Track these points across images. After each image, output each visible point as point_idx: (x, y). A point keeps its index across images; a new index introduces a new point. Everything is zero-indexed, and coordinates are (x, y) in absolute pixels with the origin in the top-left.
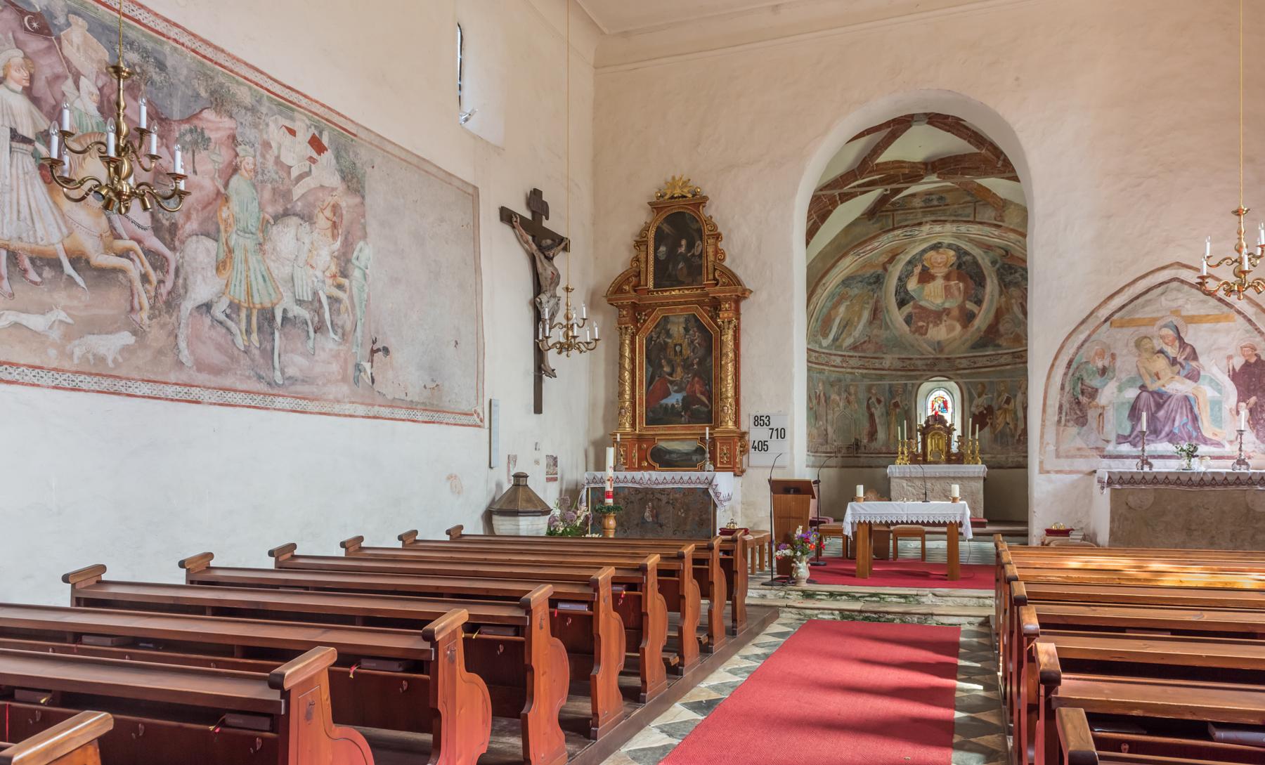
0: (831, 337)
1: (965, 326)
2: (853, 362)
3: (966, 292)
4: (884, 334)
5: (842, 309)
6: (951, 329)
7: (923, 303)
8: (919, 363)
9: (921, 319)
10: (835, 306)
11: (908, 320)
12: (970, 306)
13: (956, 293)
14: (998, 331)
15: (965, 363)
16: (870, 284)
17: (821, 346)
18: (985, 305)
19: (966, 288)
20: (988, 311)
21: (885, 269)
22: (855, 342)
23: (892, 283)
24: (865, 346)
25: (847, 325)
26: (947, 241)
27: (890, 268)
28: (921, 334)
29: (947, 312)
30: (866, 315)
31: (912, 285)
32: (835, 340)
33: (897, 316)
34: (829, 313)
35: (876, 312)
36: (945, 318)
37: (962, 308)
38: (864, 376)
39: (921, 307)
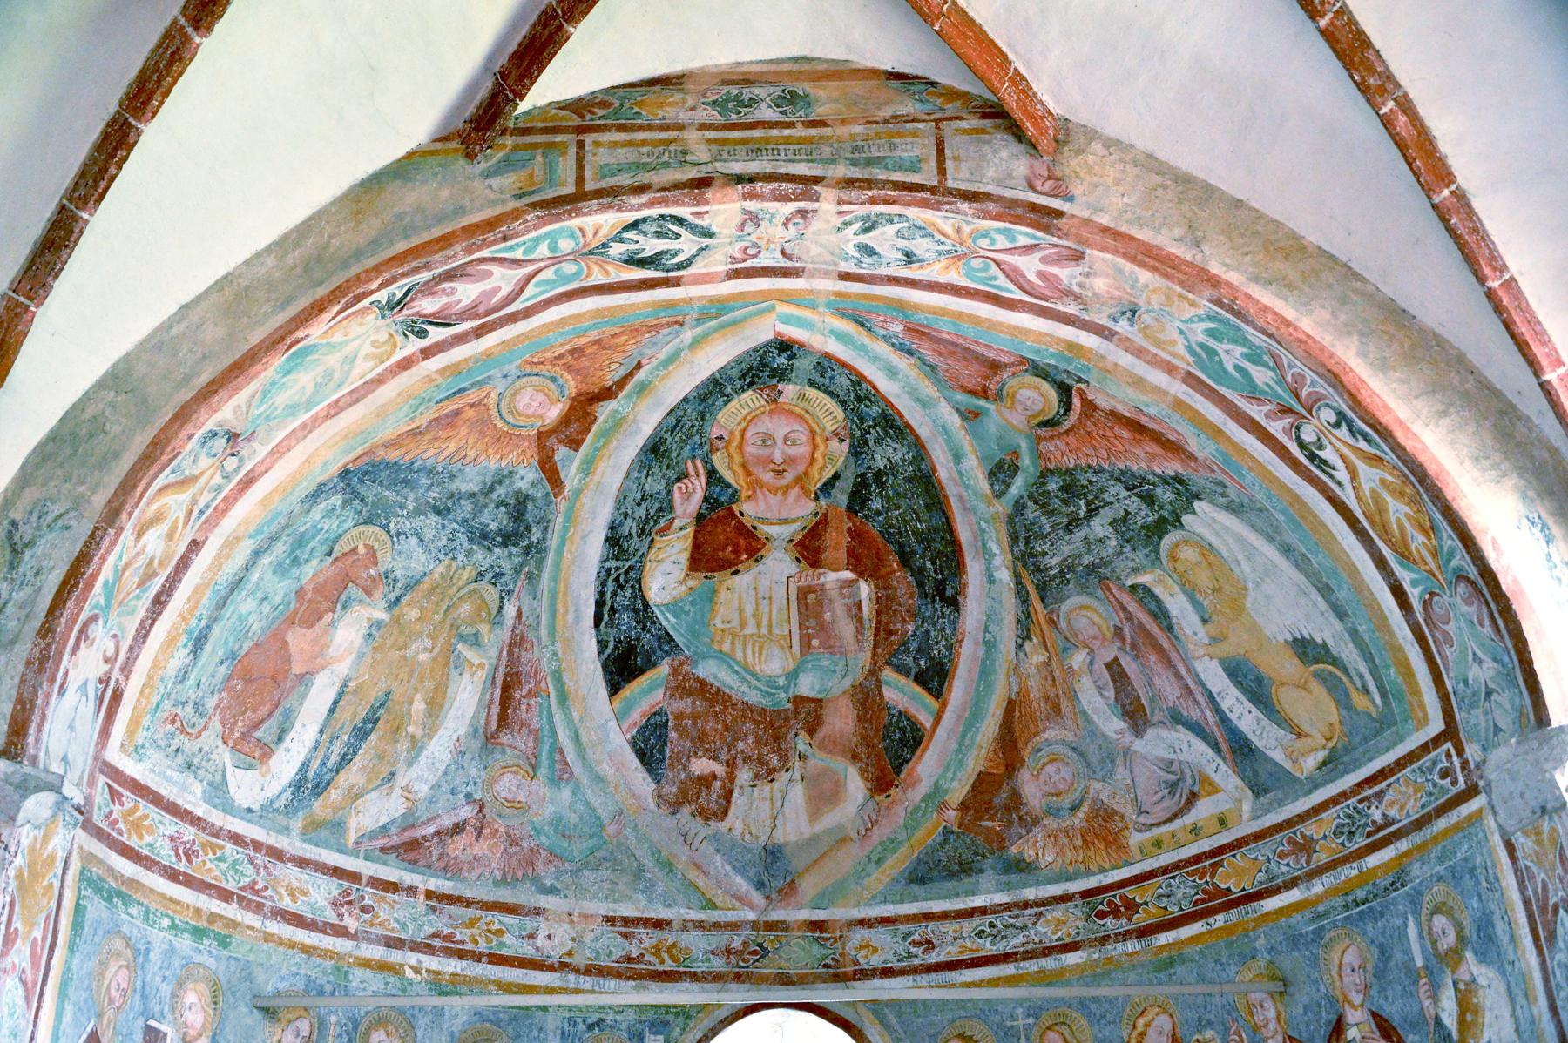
0: (286, 764)
1: (882, 784)
2: (395, 914)
3: (883, 630)
4: (549, 803)
5: (348, 633)
6: (823, 795)
7: (708, 670)
8: (698, 944)
9: (701, 744)
10: (318, 605)
11: (650, 747)
12: (900, 692)
13: (846, 629)
14: (1016, 799)
15: (886, 947)
16: (482, 537)
17: (218, 791)
18: (958, 690)
19: (885, 603)
20: (975, 711)
21: (555, 481)
22: (408, 821)
23: (581, 557)
24: (457, 847)
25: (368, 724)
26: (823, 334)
27: (571, 465)
28: (703, 814)
29: (810, 713)
30: (468, 697)
31: (666, 577)
32: (309, 786)
33: (601, 723)
34: (276, 639)
35: (509, 690)
36: (802, 743)
37: (867, 698)
38: (442, 986)
39: (702, 688)
